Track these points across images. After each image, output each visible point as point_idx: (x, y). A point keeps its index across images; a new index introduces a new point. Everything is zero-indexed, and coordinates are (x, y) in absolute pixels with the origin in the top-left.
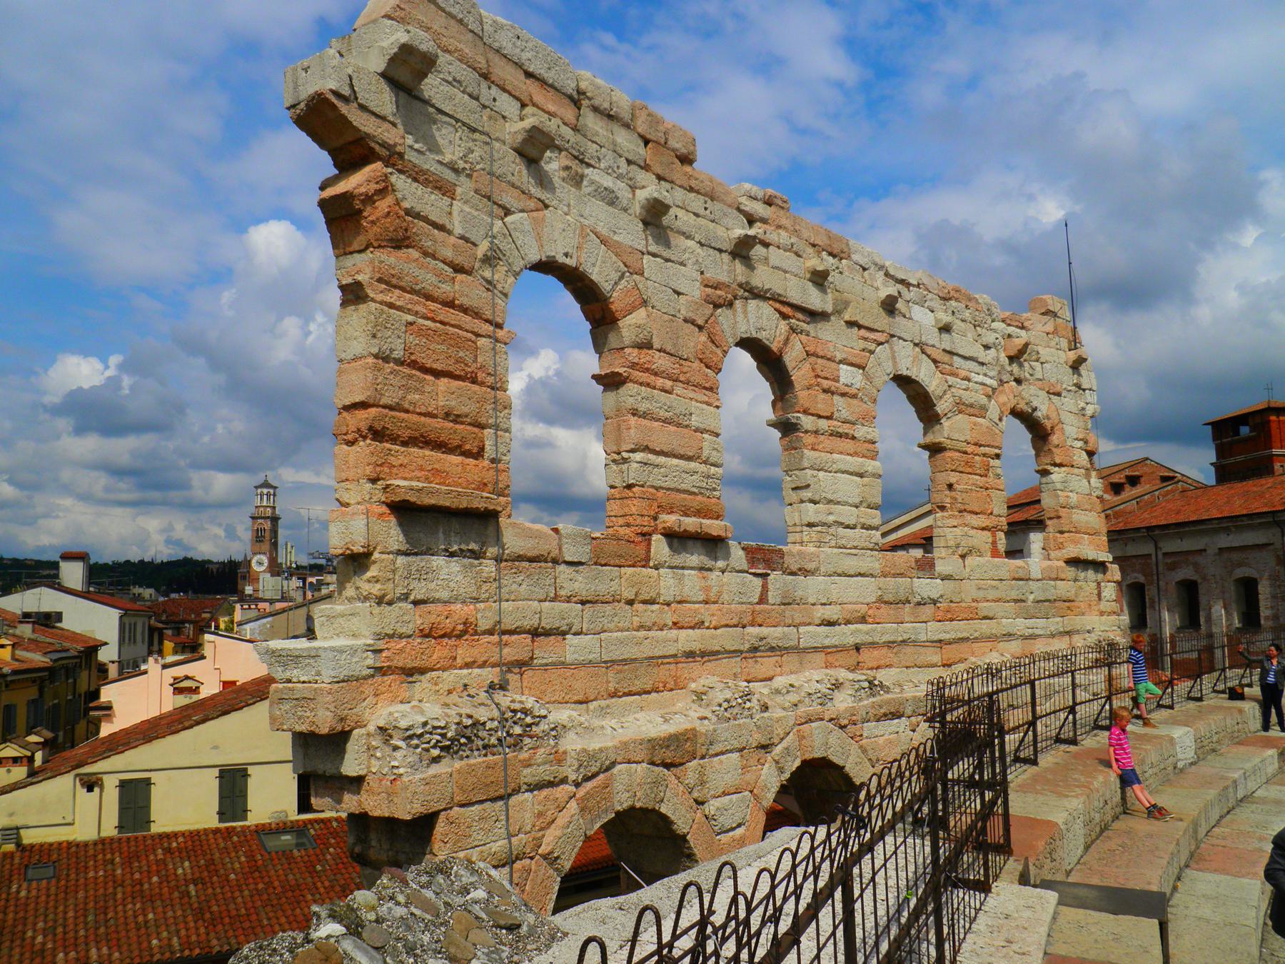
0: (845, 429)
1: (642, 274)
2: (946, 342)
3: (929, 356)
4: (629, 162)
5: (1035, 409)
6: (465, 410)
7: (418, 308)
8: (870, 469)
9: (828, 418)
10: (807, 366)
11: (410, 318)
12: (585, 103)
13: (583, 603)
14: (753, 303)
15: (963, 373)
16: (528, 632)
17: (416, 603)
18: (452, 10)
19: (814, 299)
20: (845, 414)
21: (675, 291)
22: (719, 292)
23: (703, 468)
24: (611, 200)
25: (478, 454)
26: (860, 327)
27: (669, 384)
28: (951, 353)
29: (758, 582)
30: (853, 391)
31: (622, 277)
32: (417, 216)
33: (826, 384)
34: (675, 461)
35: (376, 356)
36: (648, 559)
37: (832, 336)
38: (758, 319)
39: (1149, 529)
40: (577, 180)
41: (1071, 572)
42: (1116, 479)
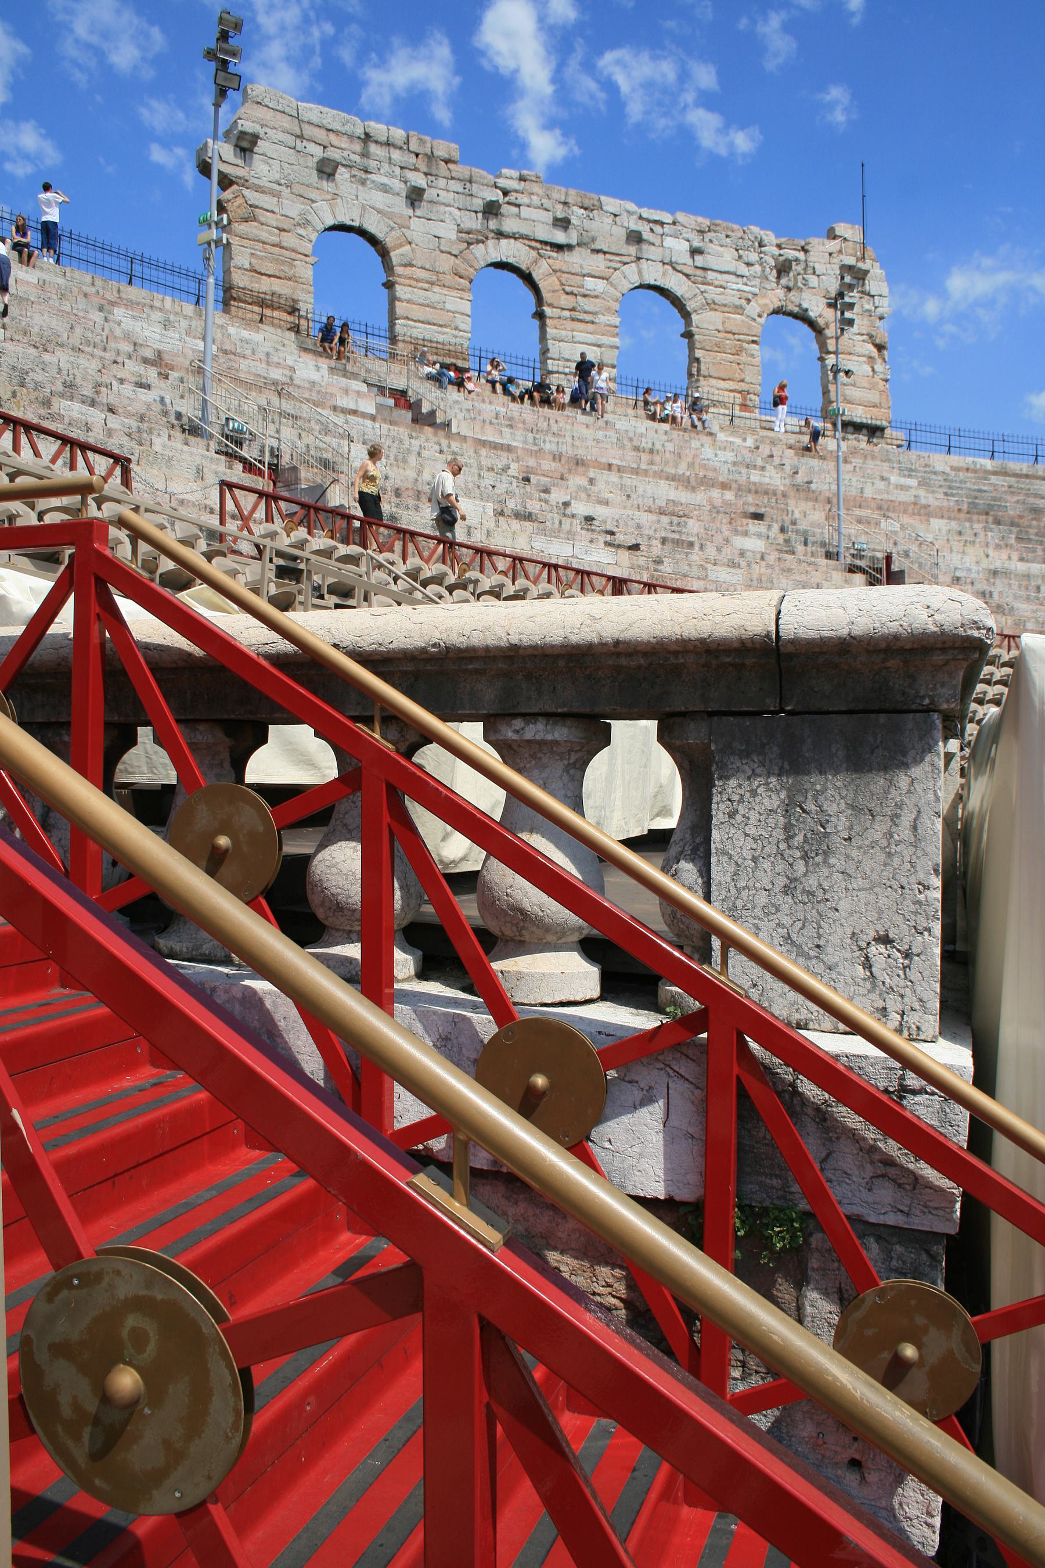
0: (588, 318)
1: (409, 228)
2: (699, 260)
4: (402, 168)
5: (807, 310)
19: (560, 237)
24: (385, 189)
26: (605, 253)
27: (426, 286)
28: (704, 269)
30: (596, 293)
32: (257, 207)
37: (577, 259)
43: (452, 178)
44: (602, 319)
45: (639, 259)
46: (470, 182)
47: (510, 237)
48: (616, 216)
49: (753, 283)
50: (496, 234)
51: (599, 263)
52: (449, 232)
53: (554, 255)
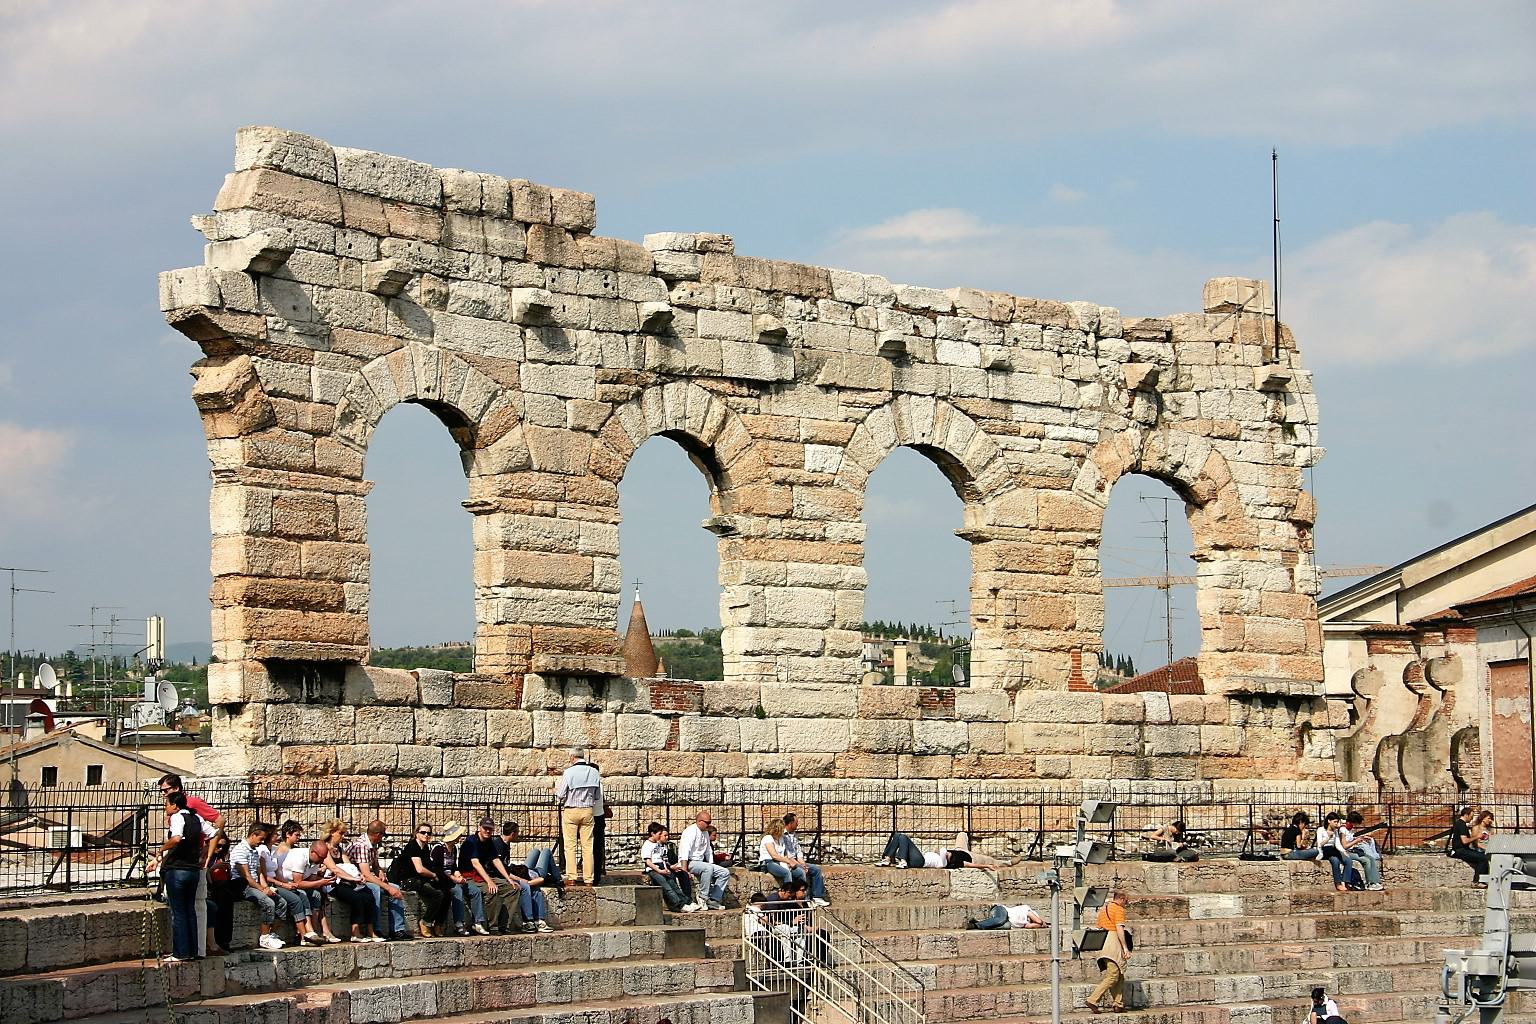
0: (814, 529)
2: (999, 385)
3: (965, 412)
4: (504, 260)
6: (325, 568)
7: (283, 481)
9: (783, 517)
10: (753, 453)
11: (276, 492)
12: (451, 207)
13: (443, 745)
14: (671, 387)
15: (1026, 429)
16: (385, 773)
17: (283, 745)
18: (307, 171)
19: (766, 365)
20: (808, 510)
21: (559, 397)
22: (619, 387)
23: (594, 596)
24: (482, 311)
25: (340, 606)
26: (841, 389)
29: (664, 725)
30: (826, 477)
31: (494, 396)
33: (779, 473)
34: (555, 592)
35: (248, 533)
36: (518, 701)
40: (442, 301)
41: (1236, 711)
44: (834, 530)
45: (896, 394)
46: (615, 270)
47: (681, 377)
48: (855, 306)
49: (1087, 422)
50: (661, 374)
51: (832, 411)
52: (580, 383)
53: (752, 403)
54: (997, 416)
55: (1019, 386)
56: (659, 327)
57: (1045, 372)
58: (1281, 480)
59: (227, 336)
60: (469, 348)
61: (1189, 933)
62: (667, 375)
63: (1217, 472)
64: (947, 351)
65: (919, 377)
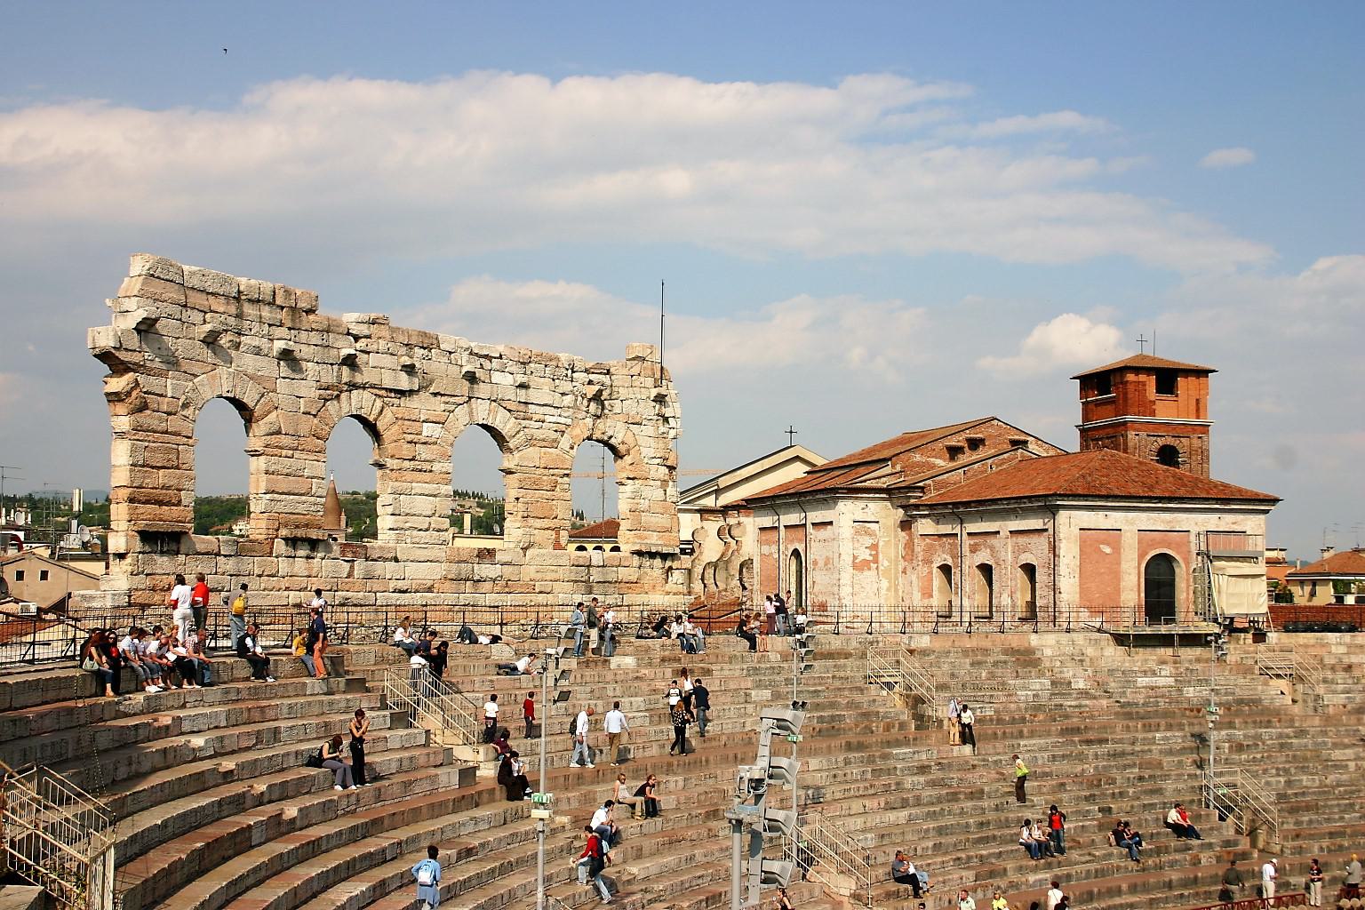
0: (426, 466)
3: (505, 408)
4: (270, 325)
7: (150, 438)
8: (299, 535)
9: (410, 460)
10: (396, 427)
11: (147, 444)
12: (243, 297)
13: (231, 575)
14: (355, 392)
15: (536, 417)
17: (147, 575)
18: (168, 277)
19: (404, 382)
20: (424, 457)
21: (297, 397)
23: (313, 499)
24: (258, 351)
25: (179, 503)
26: (442, 395)
30: (433, 440)
31: (263, 396)
33: (409, 437)
34: (292, 497)
35: (131, 465)
36: (271, 553)
38: (363, 401)
39: (956, 505)
40: (237, 346)
41: (636, 560)
42: (953, 442)
43: (313, 330)
44: (437, 467)
45: (470, 398)
47: (360, 387)
48: (450, 353)
49: (566, 415)
50: (350, 386)
51: (438, 405)
52: (308, 390)
53: (396, 401)
54: (521, 411)
55: (533, 395)
56: (350, 361)
57: (546, 388)
58: (661, 445)
59: (123, 362)
60: (250, 371)
61: (610, 677)
62: (353, 386)
63: (630, 441)
64: (496, 377)
65: (482, 390)
